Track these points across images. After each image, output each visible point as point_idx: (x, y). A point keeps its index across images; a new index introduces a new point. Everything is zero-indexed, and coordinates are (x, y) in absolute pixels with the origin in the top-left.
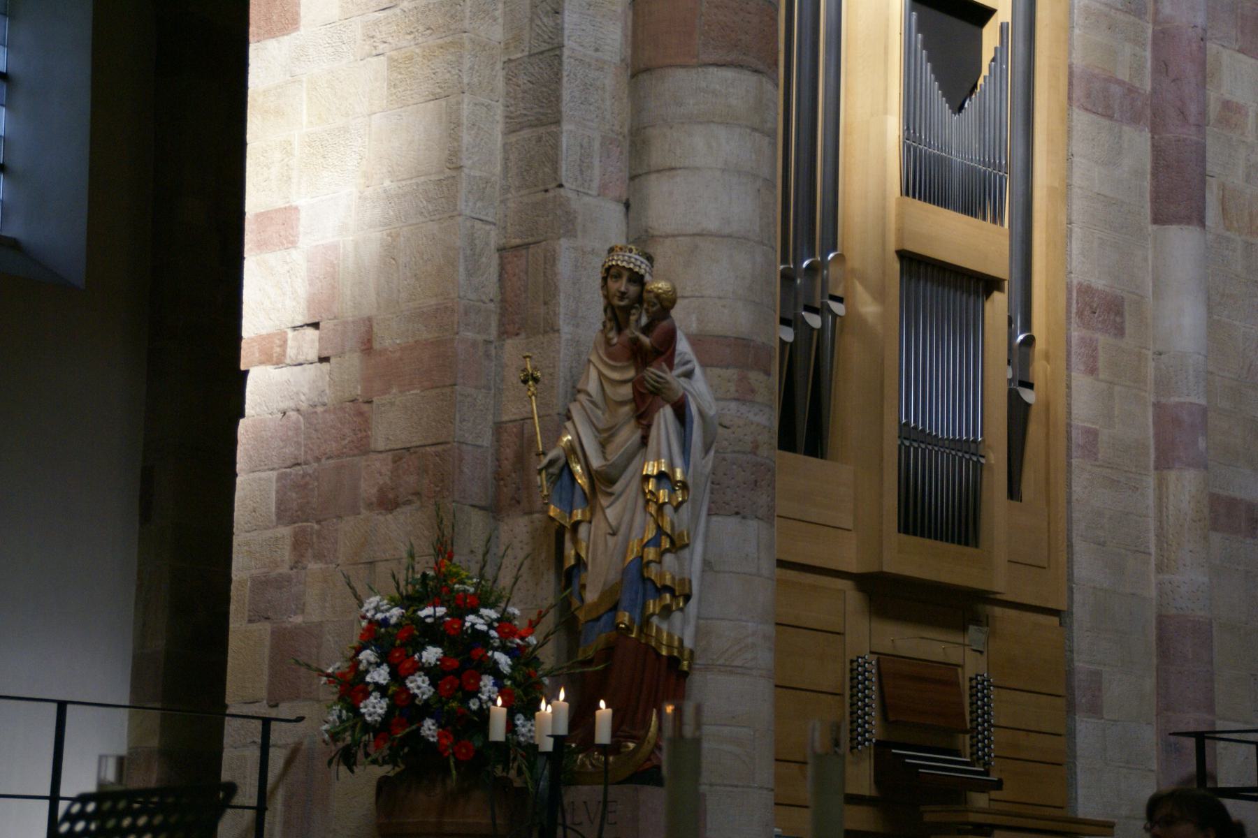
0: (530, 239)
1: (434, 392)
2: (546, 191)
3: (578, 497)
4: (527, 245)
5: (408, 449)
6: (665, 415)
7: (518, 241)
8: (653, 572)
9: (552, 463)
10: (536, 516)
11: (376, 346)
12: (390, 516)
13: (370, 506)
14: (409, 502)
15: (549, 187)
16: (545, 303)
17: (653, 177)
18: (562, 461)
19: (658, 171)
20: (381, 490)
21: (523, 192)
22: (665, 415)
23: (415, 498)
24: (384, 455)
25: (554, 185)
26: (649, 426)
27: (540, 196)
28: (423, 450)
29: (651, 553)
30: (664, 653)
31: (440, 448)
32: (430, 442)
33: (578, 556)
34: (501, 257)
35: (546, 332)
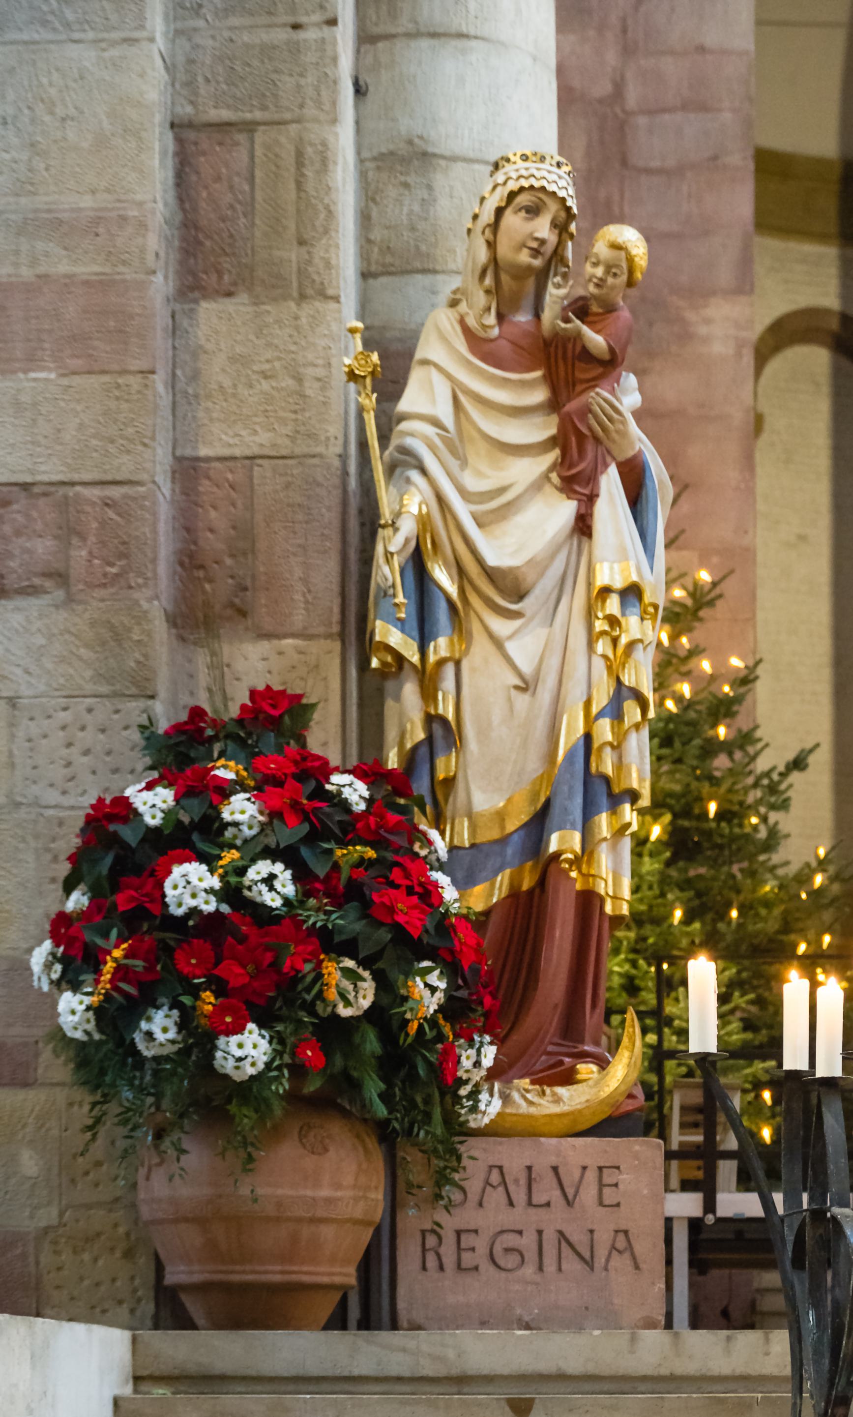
0: (258, 115)
1: (94, 382)
2: (296, 27)
4: (249, 127)
5: (25, 487)
6: (610, 482)
7: (226, 115)
9: (407, 541)
10: (290, 641)
14: (32, 591)
15: (303, 19)
18: (413, 544)
21: (235, 21)
22: (610, 482)
23: (48, 584)
25: (316, 17)
26: (590, 499)
28: (62, 491)
29: (604, 730)
31: (115, 492)
32: (86, 477)
33: (431, 720)
34: (179, 141)
35: (303, 297)
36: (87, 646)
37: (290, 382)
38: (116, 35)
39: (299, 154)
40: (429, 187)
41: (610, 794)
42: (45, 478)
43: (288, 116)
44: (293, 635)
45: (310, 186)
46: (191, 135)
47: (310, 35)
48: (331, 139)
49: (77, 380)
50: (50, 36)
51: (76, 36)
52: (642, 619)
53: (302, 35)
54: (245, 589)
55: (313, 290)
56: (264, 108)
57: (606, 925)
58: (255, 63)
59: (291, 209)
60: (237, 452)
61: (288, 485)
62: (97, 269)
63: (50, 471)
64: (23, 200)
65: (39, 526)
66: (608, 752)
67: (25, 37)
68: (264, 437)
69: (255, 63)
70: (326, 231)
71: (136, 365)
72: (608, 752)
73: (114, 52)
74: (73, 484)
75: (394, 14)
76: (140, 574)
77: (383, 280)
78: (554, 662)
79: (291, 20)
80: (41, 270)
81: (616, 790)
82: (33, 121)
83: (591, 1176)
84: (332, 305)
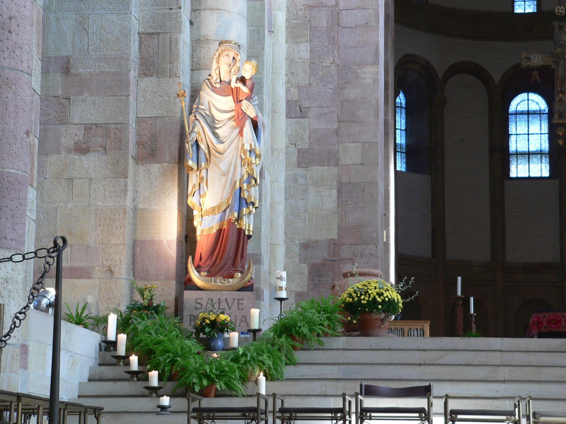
0: (160, 31)
2: (171, 9)
3: (202, 156)
4: (158, 34)
5: (96, 125)
7: (152, 31)
8: (245, 195)
11: (73, 71)
12: (82, 157)
13: (69, 151)
15: (173, 7)
16: (170, 63)
17: (208, 11)
19: (211, 9)
20: (76, 143)
23: (101, 149)
24: (79, 126)
27: (167, 11)
29: (245, 186)
30: (247, 233)
31: (119, 126)
32: (111, 122)
34: (140, 37)
36: (110, 165)
37: (167, 98)
38: (122, 12)
39: (170, 40)
40: (209, 48)
41: (247, 203)
42: (101, 122)
43: (168, 31)
44: (166, 162)
45: (173, 49)
46: (143, 36)
47: (174, 11)
48: (179, 37)
49: (109, 98)
50: (106, 12)
51: (112, 12)
52: (256, 158)
53: (172, 11)
54: (154, 150)
55: (173, 74)
56: (162, 29)
57: (246, 237)
58: (160, 18)
59: (168, 54)
60: (153, 116)
61: (165, 124)
62: (116, 70)
63: (101, 121)
64: (97, 53)
65: (99, 135)
66: (246, 192)
67: (99, 12)
68: (160, 112)
69: (160, 18)
70: (177, 60)
71: (124, 94)
72: (246, 192)
73: (122, 16)
74: (108, 124)
75: (200, 4)
76: (124, 146)
77: (197, 71)
78: (232, 169)
79: (169, 7)
80: (101, 70)
81: (248, 202)
82: (100, 33)
83: (236, 301)
84: (178, 79)
